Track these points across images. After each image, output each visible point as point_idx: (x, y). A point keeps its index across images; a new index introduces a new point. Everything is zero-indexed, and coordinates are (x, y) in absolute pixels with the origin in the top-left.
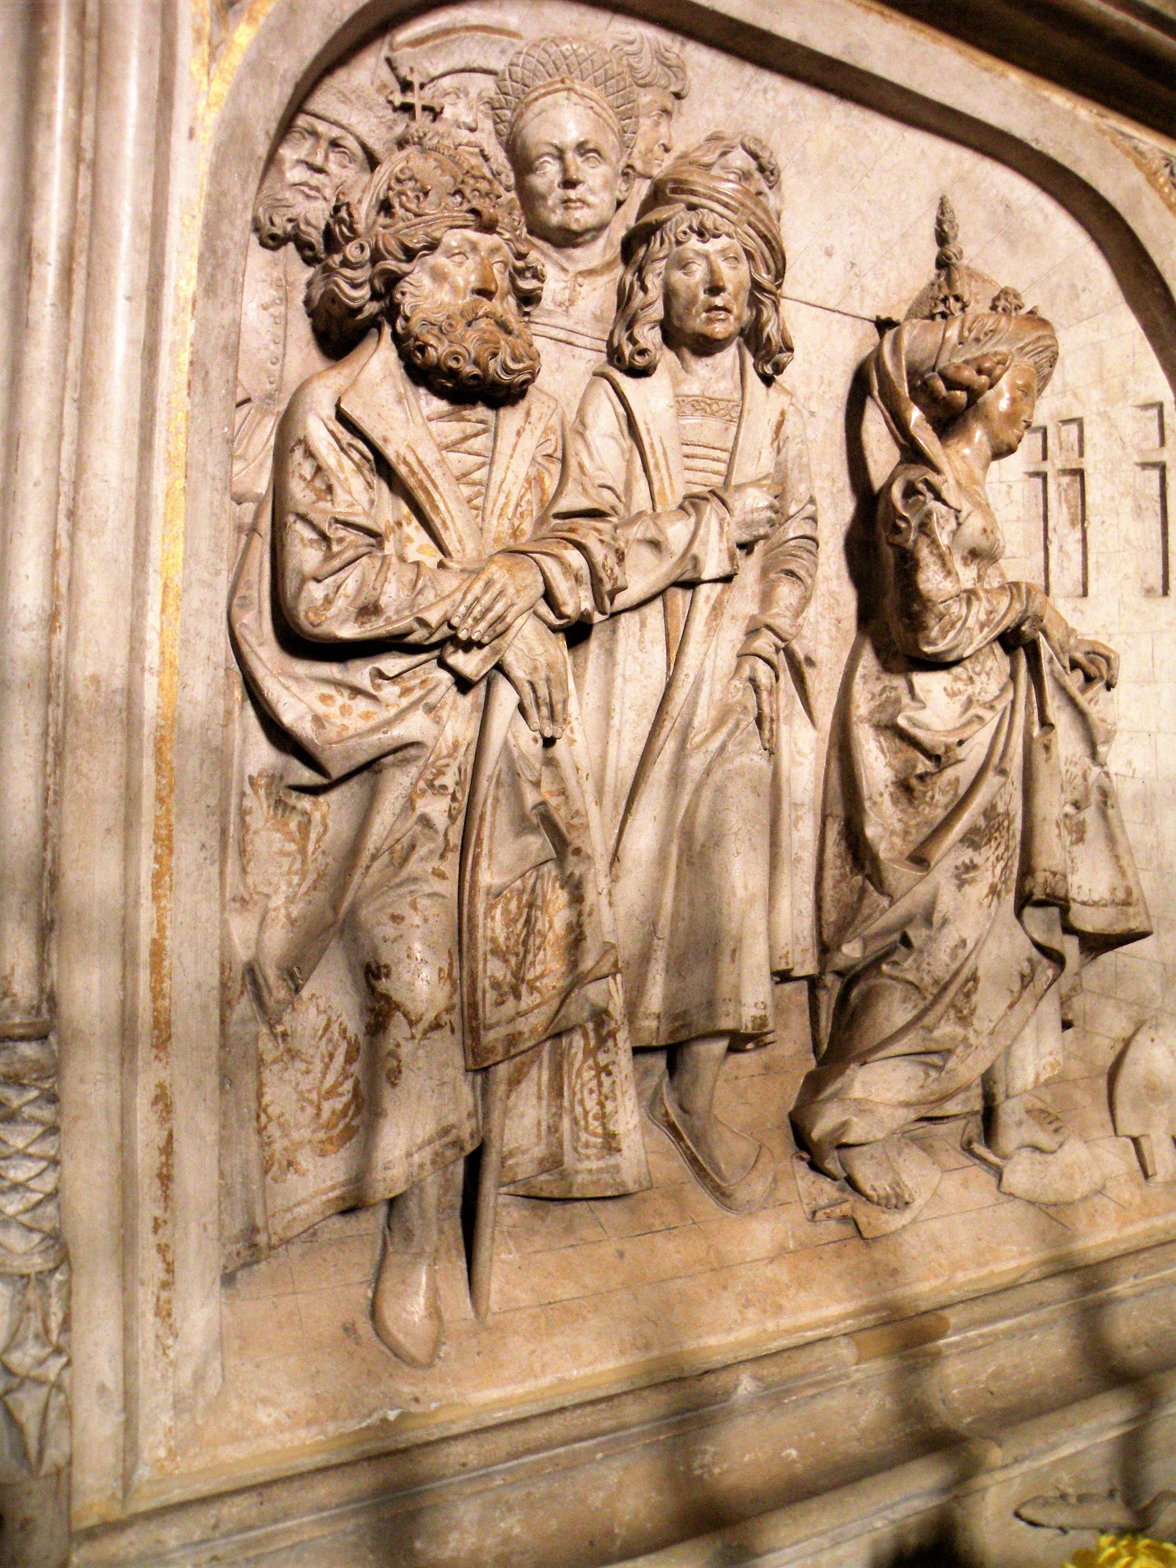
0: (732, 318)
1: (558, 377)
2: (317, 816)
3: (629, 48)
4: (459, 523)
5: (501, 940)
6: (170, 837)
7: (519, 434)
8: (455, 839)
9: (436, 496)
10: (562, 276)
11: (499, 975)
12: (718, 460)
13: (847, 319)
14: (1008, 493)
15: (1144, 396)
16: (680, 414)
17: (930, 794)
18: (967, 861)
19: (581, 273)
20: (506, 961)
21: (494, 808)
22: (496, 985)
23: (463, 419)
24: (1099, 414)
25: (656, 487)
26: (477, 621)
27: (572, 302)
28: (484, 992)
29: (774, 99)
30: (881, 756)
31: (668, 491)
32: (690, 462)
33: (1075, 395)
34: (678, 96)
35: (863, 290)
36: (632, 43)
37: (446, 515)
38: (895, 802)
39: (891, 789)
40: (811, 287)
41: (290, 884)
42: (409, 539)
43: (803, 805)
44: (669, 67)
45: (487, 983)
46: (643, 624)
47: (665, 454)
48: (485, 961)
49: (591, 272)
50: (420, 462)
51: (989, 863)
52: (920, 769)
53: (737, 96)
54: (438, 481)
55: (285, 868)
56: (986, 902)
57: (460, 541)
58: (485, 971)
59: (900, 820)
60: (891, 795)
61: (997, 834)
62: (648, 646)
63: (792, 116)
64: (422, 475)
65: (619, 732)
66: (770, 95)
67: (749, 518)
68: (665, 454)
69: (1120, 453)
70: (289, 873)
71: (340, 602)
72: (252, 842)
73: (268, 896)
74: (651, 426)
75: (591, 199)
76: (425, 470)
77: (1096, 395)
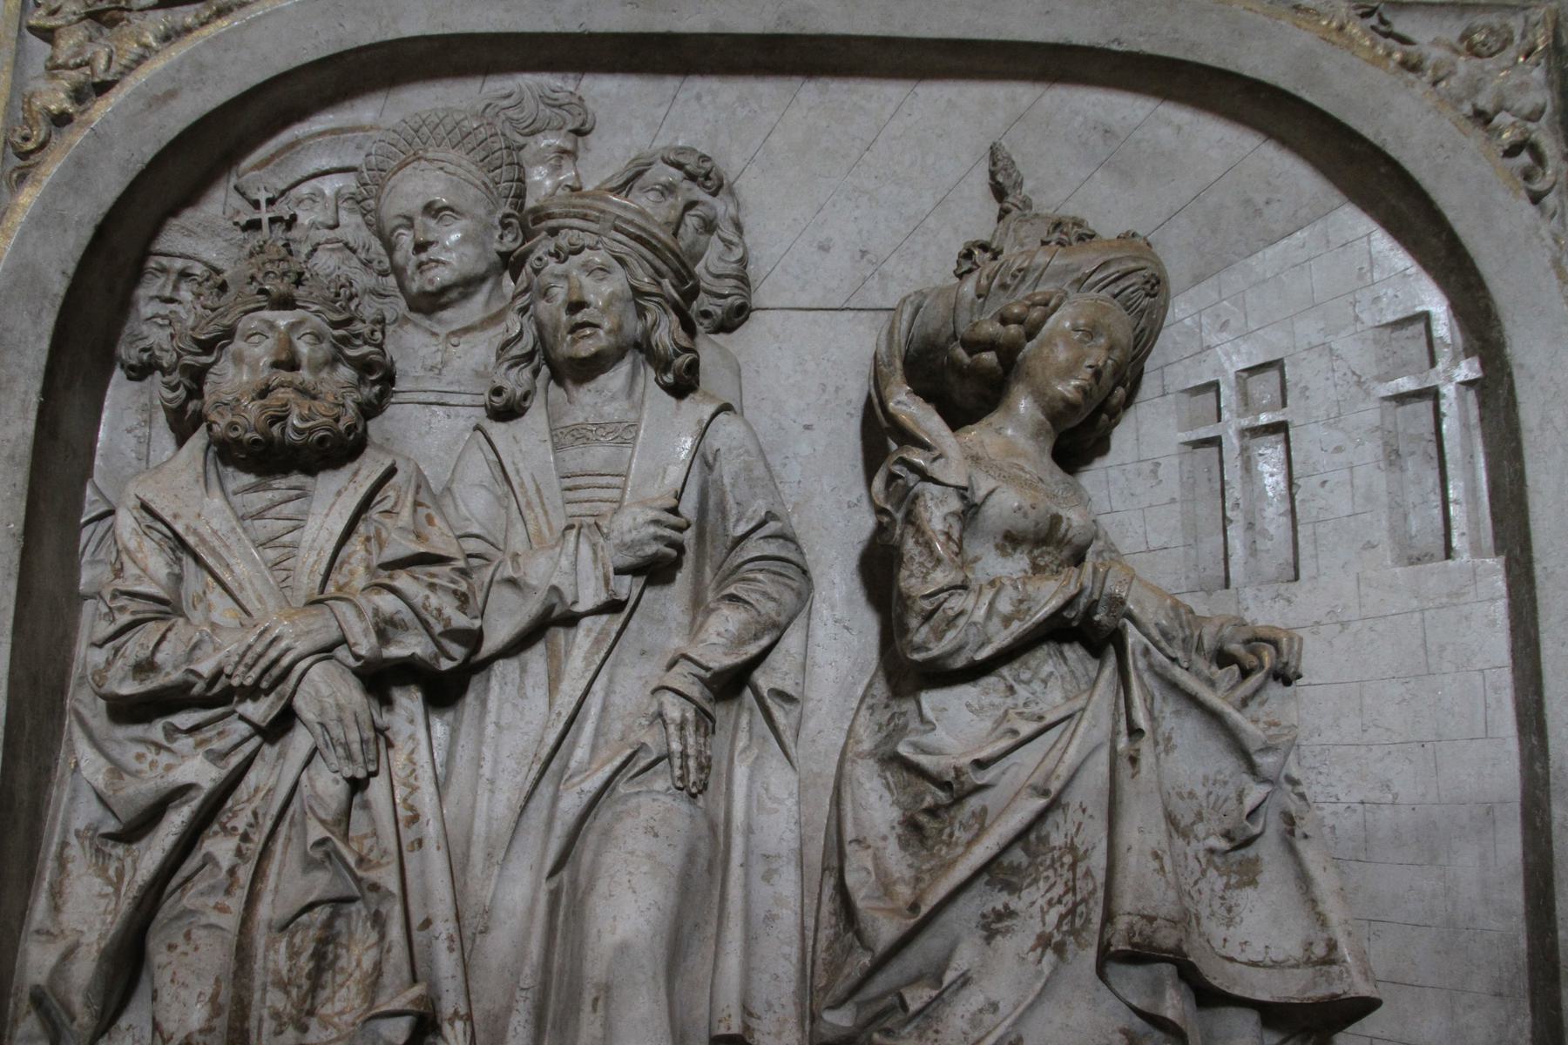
0: (601, 333)
3: (506, 103)
5: (284, 972)
8: (245, 874)
10: (433, 341)
11: (280, 1006)
13: (864, 314)
16: (557, 448)
17: (947, 831)
18: (1000, 907)
19: (454, 333)
20: (288, 993)
22: (276, 1015)
25: (531, 528)
27: (444, 363)
28: (261, 1020)
30: (887, 794)
32: (571, 495)
34: (579, 132)
35: (883, 276)
36: (509, 96)
38: (904, 845)
39: (899, 830)
40: (803, 289)
44: (560, 107)
45: (265, 1013)
46: (523, 670)
47: (538, 490)
48: (264, 990)
49: (467, 330)
51: (1036, 910)
52: (928, 801)
56: (1032, 957)
58: (263, 1000)
60: (899, 837)
61: (1050, 873)
65: (492, 782)
67: (628, 538)
68: (538, 490)
74: (521, 465)
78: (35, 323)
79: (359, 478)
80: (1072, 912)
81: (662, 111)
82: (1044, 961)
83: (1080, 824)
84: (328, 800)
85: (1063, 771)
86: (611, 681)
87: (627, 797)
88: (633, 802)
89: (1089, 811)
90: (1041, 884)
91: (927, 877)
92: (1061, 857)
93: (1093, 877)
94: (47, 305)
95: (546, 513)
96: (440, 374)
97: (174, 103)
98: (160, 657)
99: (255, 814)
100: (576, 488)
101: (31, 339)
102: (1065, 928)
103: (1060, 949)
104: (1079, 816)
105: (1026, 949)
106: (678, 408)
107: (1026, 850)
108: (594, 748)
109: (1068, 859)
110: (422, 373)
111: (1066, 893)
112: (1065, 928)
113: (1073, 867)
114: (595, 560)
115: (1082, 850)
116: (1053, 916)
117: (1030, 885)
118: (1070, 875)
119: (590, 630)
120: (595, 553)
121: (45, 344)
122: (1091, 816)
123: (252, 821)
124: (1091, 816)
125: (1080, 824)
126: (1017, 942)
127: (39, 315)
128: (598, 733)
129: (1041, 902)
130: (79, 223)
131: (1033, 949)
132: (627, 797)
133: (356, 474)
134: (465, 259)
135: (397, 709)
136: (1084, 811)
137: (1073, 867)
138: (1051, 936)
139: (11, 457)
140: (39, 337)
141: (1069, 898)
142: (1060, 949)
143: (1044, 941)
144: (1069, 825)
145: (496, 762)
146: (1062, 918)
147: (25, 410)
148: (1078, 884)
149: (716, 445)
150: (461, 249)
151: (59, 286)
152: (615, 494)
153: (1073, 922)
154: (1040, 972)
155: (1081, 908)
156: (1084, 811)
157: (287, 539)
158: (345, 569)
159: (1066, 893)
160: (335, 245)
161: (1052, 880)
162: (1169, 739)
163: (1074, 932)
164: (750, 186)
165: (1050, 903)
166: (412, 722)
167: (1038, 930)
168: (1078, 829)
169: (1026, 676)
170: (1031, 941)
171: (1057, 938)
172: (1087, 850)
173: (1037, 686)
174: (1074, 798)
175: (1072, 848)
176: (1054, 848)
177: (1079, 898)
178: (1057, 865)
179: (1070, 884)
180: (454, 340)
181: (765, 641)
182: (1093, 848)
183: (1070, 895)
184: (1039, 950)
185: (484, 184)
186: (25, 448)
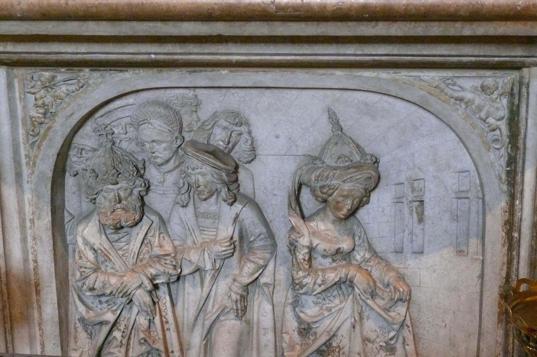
1: (162, 204)
2: (93, 331)
4: (119, 263)
6: (44, 344)
7: (138, 234)
8: (125, 341)
9: (111, 257)
12: (212, 231)
14: (383, 211)
15: (459, 167)
21: (134, 336)
23: (119, 233)
24: (434, 177)
26: (119, 293)
27: (164, 182)
29: (238, 95)
31: (196, 241)
32: (202, 232)
33: (420, 169)
35: (297, 146)
37: (114, 262)
41: (89, 345)
42: (107, 266)
43: (267, 329)
46: (194, 278)
47: (193, 230)
50: (105, 249)
53: (222, 98)
54: (111, 253)
55: (88, 342)
57: (120, 267)
59: (300, 340)
61: (332, 353)
62: (196, 285)
63: (247, 98)
64: (106, 252)
65: (188, 309)
66: (236, 95)
68: (193, 230)
69: (445, 193)
70: (89, 343)
71: (85, 287)
72: (79, 335)
73: (83, 348)
75: (160, 155)
76: (106, 250)
77: (431, 169)
78: (46, 188)
79: (143, 228)
81: (222, 98)
83: (341, 340)
84: (144, 325)
85: (338, 324)
86: (217, 286)
87: (222, 321)
88: (224, 322)
89: (344, 336)
91: (304, 345)
94: (48, 181)
95: (196, 237)
96: (163, 184)
97: (73, 116)
98: (95, 287)
99: (125, 325)
100: (204, 230)
101: (46, 192)
104: (341, 338)
106: (231, 209)
107: (326, 346)
108: (213, 306)
109: (337, 350)
110: (158, 184)
113: (339, 352)
114: (209, 258)
115: (342, 347)
118: (338, 354)
119: (210, 274)
120: (209, 256)
121: (50, 192)
122: (345, 338)
123: (125, 327)
125: (341, 340)
127: (46, 185)
128: (214, 301)
130: (53, 155)
132: (222, 321)
133: (142, 227)
134: (166, 155)
135: (160, 290)
136: (343, 336)
137: (339, 352)
139: (47, 229)
140: (48, 191)
144: (338, 340)
145: (188, 303)
147: (48, 214)
149: (243, 218)
150: (165, 153)
151: (50, 174)
152: (215, 233)
156: (343, 336)
157: (125, 248)
158: (142, 254)
160: (127, 139)
162: (368, 316)
164: (253, 119)
166: (165, 293)
168: (340, 342)
169: (329, 295)
173: (332, 298)
174: (340, 333)
175: (339, 347)
176: (333, 347)
178: (334, 351)
180: (166, 174)
181: (260, 272)
185: (169, 130)
186: (50, 225)
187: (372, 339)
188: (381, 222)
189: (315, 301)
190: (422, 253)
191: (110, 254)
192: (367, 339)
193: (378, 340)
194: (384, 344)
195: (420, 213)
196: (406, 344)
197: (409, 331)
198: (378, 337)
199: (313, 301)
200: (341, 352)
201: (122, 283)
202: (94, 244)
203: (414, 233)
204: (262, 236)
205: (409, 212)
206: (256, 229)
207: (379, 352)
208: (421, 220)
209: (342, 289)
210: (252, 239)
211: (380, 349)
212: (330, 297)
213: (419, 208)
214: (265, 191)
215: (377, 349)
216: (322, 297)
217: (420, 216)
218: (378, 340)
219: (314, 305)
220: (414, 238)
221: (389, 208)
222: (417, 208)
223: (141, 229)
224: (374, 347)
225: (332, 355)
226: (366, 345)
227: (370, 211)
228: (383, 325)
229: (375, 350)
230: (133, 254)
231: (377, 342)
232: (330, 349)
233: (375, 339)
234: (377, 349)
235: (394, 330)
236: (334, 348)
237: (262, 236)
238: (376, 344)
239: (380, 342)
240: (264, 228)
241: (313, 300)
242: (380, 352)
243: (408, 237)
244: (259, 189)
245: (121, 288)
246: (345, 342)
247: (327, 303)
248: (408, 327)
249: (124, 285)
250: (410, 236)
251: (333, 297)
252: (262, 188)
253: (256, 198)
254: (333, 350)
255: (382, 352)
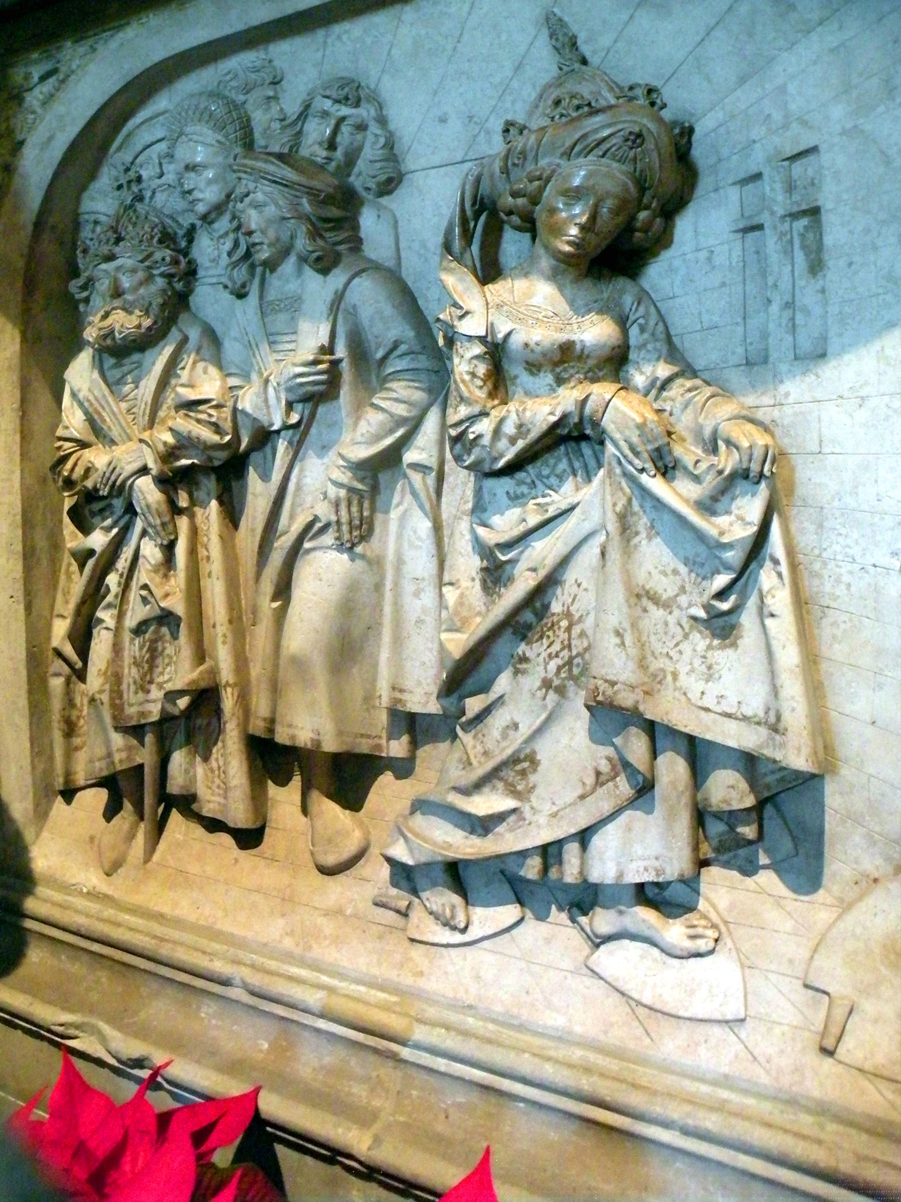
1: (216, 306)
9: (104, 414)
61: (550, 633)
80: (569, 663)
82: (548, 697)
89: (584, 585)
90: (544, 640)
92: (558, 622)
93: (587, 636)
102: (563, 675)
103: (561, 691)
104: (575, 589)
105: (535, 688)
109: (564, 623)
111: (562, 649)
112: (563, 675)
113: (569, 629)
116: (553, 665)
117: (537, 641)
118: (566, 635)
122: (586, 590)
124: (586, 590)
125: (576, 596)
126: (532, 681)
129: (544, 655)
131: (540, 689)
136: (579, 585)
137: (569, 629)
138: (551, 681)
139: (10, 367)
141: (565, 654)
142: (561, 691)
143: (547, 684)
146: (559, 669)
148: (573, 642)
153: (570, 670)
154: (545, 706)
155: (578, 660)
156: (579, 585)
159: (562, 649)
161: (552, 639)
163: (571, 677)
165: (550, 656)
167: (543, 675)
168: (574, 600)
170: (538, 683)
171: (556, 682)
172: (581, 616)
175: (568, 615)
176: (553, 614)
177: (574, 653)
178: (556, 627)
179: (566, 642)
182: (588, 614)
183: (566, 651)
184: (544, 690)
187: (665, 597)
188: (705, 290)
189: (512, 492)
190: (823, 355)
191: (103, 408)
192: (648, 592)
193: (683, 600)
194: (702, 614)
195: (814, 247)
196: (766, 611)
197: (780, 575)
198: (683, 590)
199: (508, 493)
200: (576, 631)
201: (110, 464)
202: (79, 390)
203: (798, 303)
204: (403, 348)
205: (779, 247)
206: (388, 329)
207: (686, 636)
208: (816, 266)
209: (582, 456)
210: (380, 354)
211: (691, 627)
212: (548, 477)
213: (810, 236)
214: (422, 251)
215: (681, 626)
216: (528, 480)
217: (812, 256)
218: (683, 600)
219: (510, 502)
220: (800, 318)
221: (726, 247)
222: (802, 236)
223: (160, 353)
224: (672, 620)
225: (548, 637)
226: (645, 610)
227: (677, 263)
228: (697, 555)
229: (674, 629)
230: (143, 406)
231: (679, 607)
232: (545, 621)
233: (677, 596)
234: (681, 626)
235: (728, 568)
236: (555, 619)
237: (403, 348)
238: (676, 612)
239: (690, 605)
240: (407, 327)
241: (507, 488)
242: (691, 637)
243: (780, 317)
244: (410, 247)
245: (107, 475)
246: (585, 603)
247: (540, 494)
248: (776, 562)
249: (111, 468)
250: (788, 313)
251: (557, 476)
252: (416, 246)
253: (403, 269)
254: (553, 625)
255: (696, 636)
